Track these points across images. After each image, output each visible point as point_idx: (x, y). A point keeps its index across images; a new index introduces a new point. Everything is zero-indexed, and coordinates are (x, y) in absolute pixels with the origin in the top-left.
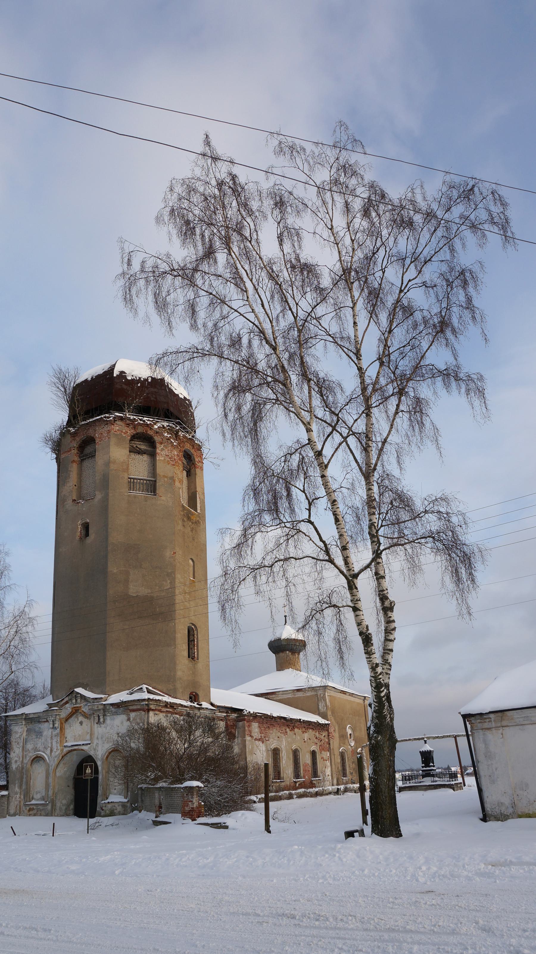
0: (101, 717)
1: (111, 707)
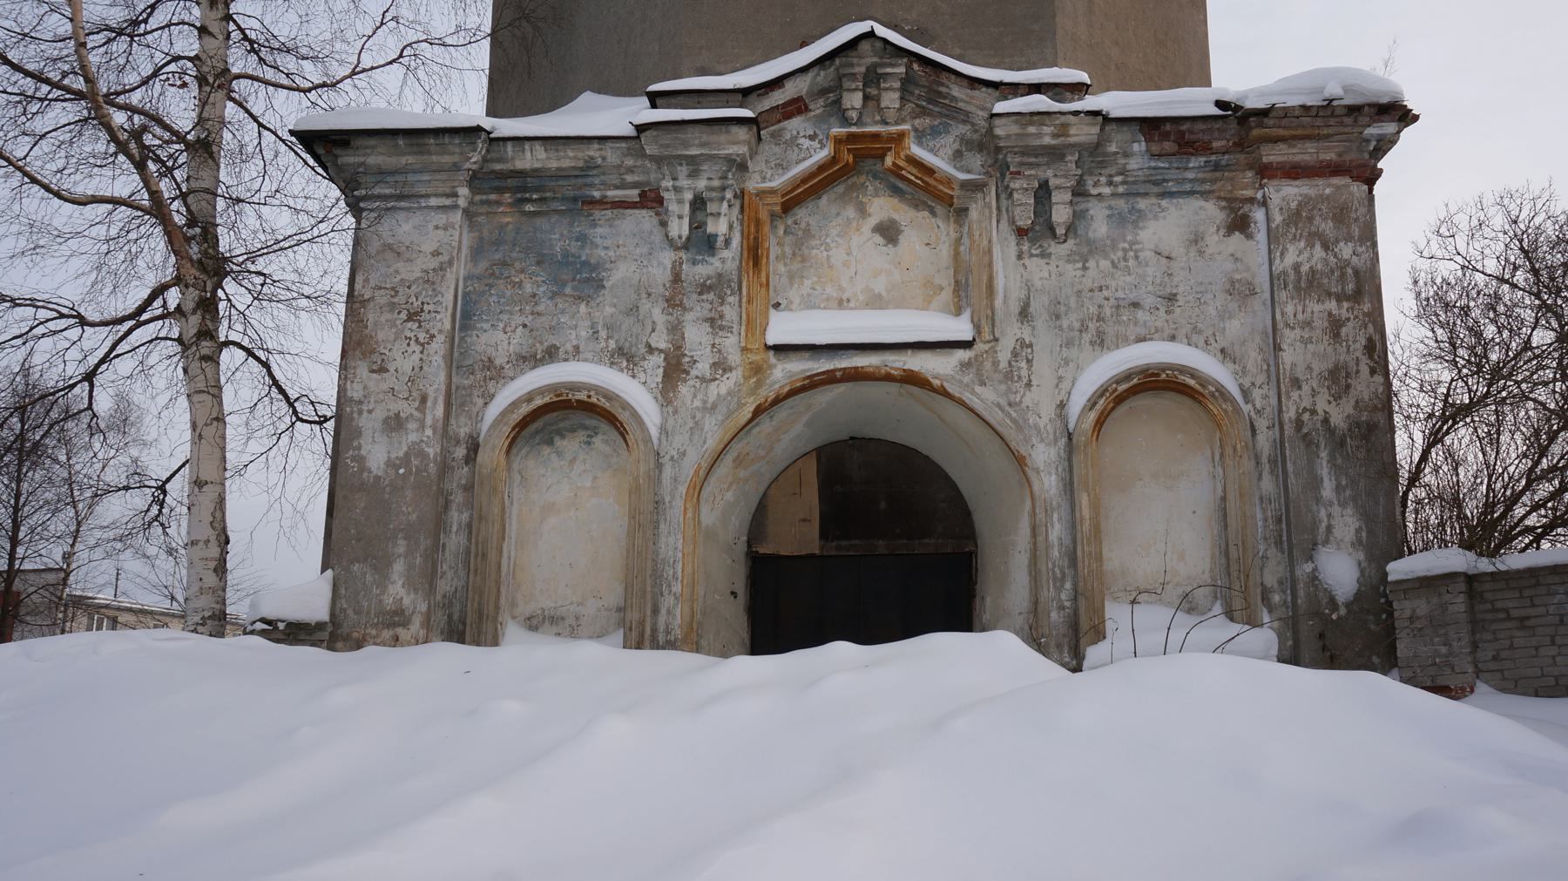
0: (1060, 198)
1: (1139, 147)
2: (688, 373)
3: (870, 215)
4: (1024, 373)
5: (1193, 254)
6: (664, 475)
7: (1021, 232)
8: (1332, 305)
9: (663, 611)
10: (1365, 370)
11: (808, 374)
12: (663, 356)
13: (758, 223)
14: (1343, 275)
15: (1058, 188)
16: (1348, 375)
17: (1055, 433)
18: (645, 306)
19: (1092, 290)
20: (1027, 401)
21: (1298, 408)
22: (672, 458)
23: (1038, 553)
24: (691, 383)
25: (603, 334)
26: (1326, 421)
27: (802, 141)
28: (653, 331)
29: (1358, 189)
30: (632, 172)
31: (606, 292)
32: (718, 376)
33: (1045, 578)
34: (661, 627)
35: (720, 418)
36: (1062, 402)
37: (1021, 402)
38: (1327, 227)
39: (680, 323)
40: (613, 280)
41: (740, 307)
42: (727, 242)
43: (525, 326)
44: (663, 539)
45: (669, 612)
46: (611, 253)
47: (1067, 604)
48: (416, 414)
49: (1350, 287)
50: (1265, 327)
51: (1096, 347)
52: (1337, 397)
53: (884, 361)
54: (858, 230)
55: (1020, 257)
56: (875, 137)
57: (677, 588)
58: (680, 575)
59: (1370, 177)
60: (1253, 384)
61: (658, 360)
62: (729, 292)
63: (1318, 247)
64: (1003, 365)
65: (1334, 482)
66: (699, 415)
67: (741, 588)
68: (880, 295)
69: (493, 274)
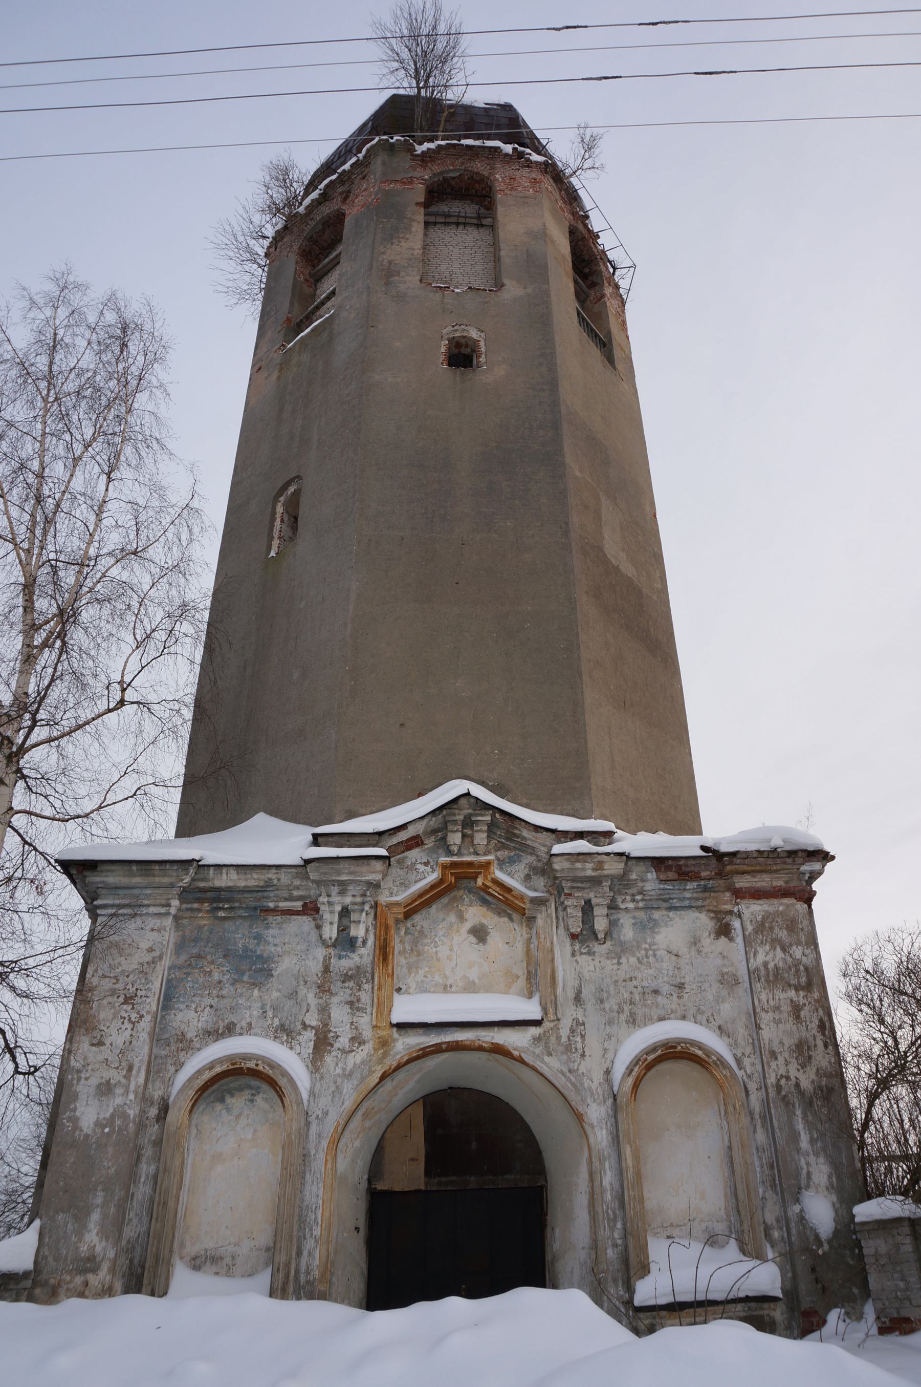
1: (651, 875)
2: (332, 1046)
3: (466, 920)
4: (579, 1046)
5: (693, 953)
6: (311, 1131)
7: (574, 937)
8: (792, 993)
9: (305, 1253)
10: (820, 1044)
11: (422, 1047)
12: (314, 1031)
13: (387, 928)
14: (797, 971)
15: (598, 905)
16: (809, 1048)
17: (604, 1094)
18: (302, 991)
19: (625, 981)
20: (582, 1069)
21: (777, 1075)
22: (318, 1117)
23: (595, 1196)
24: (334, 1054)
25: (270, 1014)
26: (797, 1085)
27: (419, 866)
28: (308, 1011)
29: (801, 907)
30: (298, 889)
31: (274, 979)
32: (355, 1048)
33: (601, 1218)
34: (303, 1268)
35: (355, 1083)
36: (607, 1069)
37: (578, 1069)
38: (783, 934)
39: (328, 1005)
40: (280, 970)
41: (373, 992)
42: (364, 942)
43: (211, 1006)
44: (308, 1188)
45: (310, 1254)
46: (279, 949)
47: (619, 1242)
48: (123, 1081)
49: (803, 980)
50: (748, 1009)
51: (630, 1025)
52: (803, 1066)
53: (477, 1036)
54: (458, 932)
55: (573, 955)
56: (470, 864)
57: (317, 1232)
58: (320, 1220)
59: (808, 897)
60: (743, 1054)
61: (310, 1035)
62: (364, 981)
63: (778, 950)
64: (564, 1039)
65: (808, 1136)
66: (339, 1080)
67: (362, 1224)
68: (473, 982)
69: (190, 965)
